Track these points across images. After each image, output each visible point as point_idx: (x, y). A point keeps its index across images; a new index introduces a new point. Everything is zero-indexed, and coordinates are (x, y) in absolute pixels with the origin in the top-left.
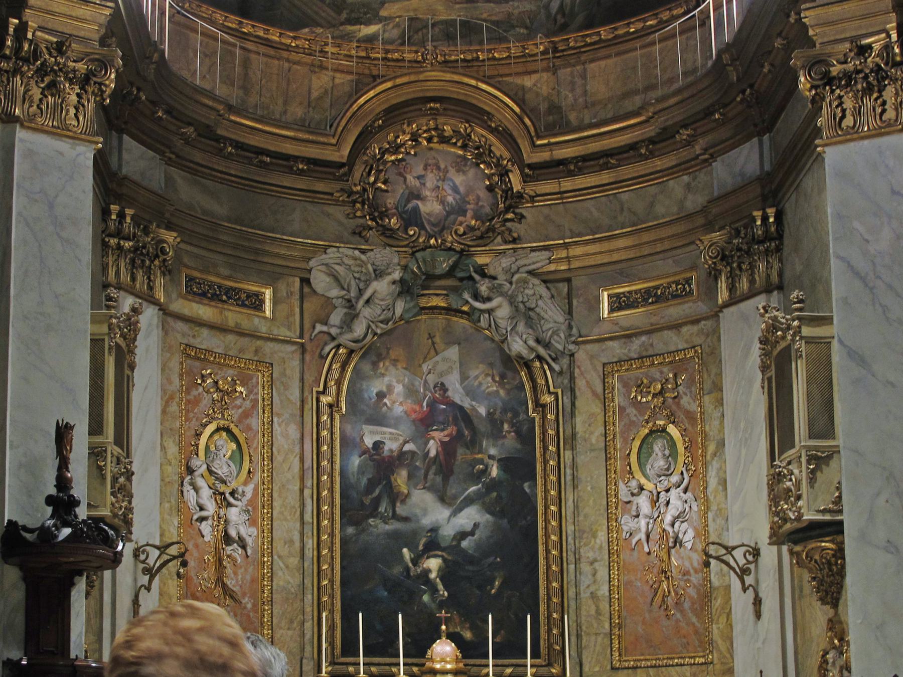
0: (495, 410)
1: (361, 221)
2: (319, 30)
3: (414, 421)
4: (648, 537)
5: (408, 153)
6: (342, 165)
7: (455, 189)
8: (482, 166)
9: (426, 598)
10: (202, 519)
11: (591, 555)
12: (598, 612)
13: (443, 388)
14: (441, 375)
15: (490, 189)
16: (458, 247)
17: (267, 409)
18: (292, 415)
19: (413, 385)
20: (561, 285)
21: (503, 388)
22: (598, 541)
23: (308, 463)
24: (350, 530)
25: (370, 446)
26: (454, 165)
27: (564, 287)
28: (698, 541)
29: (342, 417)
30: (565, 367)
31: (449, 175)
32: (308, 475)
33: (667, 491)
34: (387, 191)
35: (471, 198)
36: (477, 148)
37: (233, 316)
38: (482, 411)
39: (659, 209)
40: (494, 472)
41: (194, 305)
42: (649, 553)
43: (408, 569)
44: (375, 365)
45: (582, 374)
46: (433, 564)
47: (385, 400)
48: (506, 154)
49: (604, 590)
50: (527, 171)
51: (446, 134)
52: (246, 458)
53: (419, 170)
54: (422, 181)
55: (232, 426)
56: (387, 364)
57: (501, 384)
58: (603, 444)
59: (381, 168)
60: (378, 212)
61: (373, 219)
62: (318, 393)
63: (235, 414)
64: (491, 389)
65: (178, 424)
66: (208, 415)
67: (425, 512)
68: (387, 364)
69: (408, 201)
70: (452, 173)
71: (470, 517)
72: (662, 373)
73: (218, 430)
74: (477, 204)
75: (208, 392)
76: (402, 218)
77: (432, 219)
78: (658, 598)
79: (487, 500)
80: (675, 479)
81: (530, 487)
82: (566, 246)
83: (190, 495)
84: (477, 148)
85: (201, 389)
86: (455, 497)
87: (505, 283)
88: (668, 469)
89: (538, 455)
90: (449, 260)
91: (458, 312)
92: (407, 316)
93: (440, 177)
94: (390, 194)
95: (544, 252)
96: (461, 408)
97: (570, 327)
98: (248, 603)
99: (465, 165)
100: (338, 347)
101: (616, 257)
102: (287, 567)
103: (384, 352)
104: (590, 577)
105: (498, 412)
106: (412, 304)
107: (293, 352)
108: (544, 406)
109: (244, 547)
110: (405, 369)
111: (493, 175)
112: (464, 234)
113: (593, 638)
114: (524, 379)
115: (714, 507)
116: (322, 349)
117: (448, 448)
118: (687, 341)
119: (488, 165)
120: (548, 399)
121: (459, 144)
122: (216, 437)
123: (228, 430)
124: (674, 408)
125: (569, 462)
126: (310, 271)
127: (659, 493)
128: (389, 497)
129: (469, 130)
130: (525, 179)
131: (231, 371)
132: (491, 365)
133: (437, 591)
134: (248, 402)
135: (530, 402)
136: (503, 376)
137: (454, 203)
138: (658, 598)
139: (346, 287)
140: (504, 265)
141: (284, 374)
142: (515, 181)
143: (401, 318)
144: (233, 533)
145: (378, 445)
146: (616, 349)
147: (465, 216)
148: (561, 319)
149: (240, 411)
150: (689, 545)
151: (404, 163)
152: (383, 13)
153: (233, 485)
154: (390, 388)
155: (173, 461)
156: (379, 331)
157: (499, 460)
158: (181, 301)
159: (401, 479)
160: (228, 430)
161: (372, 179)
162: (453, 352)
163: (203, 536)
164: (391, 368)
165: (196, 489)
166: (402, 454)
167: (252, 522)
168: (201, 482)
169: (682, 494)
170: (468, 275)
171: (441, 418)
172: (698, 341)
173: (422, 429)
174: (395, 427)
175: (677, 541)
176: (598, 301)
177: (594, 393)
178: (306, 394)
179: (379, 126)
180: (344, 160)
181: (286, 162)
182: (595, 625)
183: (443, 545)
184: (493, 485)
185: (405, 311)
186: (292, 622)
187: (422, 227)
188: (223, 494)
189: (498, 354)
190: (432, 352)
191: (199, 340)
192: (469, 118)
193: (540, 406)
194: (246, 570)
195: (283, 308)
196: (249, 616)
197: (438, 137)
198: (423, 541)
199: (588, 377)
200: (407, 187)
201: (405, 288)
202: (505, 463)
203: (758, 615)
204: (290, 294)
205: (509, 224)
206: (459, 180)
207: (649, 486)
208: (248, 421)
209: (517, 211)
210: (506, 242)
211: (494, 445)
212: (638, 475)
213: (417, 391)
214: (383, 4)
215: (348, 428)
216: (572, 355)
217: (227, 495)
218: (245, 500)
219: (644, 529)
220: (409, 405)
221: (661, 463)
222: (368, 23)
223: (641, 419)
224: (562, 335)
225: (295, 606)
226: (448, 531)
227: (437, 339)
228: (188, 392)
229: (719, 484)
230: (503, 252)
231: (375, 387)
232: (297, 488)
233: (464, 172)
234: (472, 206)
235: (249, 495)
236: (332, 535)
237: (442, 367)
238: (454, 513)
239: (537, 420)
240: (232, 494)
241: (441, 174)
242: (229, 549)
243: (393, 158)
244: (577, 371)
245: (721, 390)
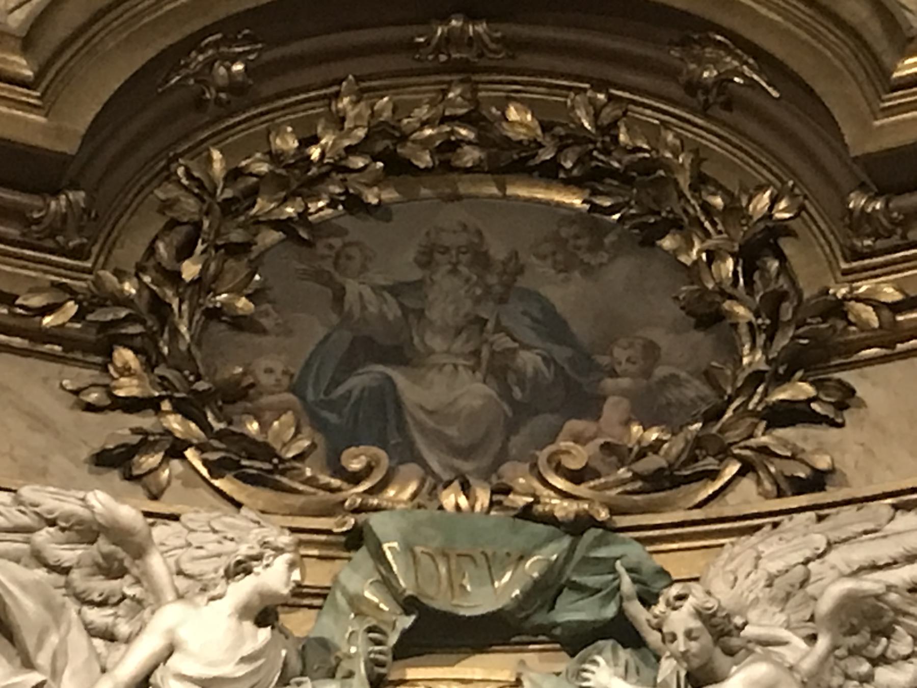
26: (547, 248)
54: (410, 303)
74: (647, 374)
77: (452, 431)
87: (785, 634)
90: (522, 558)
93: (488, 289)
99: (596, 247)
137: (548, 374)
151: (337, 242)
170: (610, 611)
179: (235, 87)
192: (611, 72)
197: (479, 143)
200: (346, 318)
233: (588, 270)
241: (492, 279)
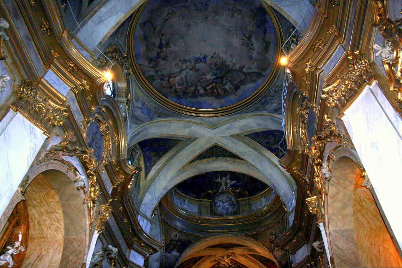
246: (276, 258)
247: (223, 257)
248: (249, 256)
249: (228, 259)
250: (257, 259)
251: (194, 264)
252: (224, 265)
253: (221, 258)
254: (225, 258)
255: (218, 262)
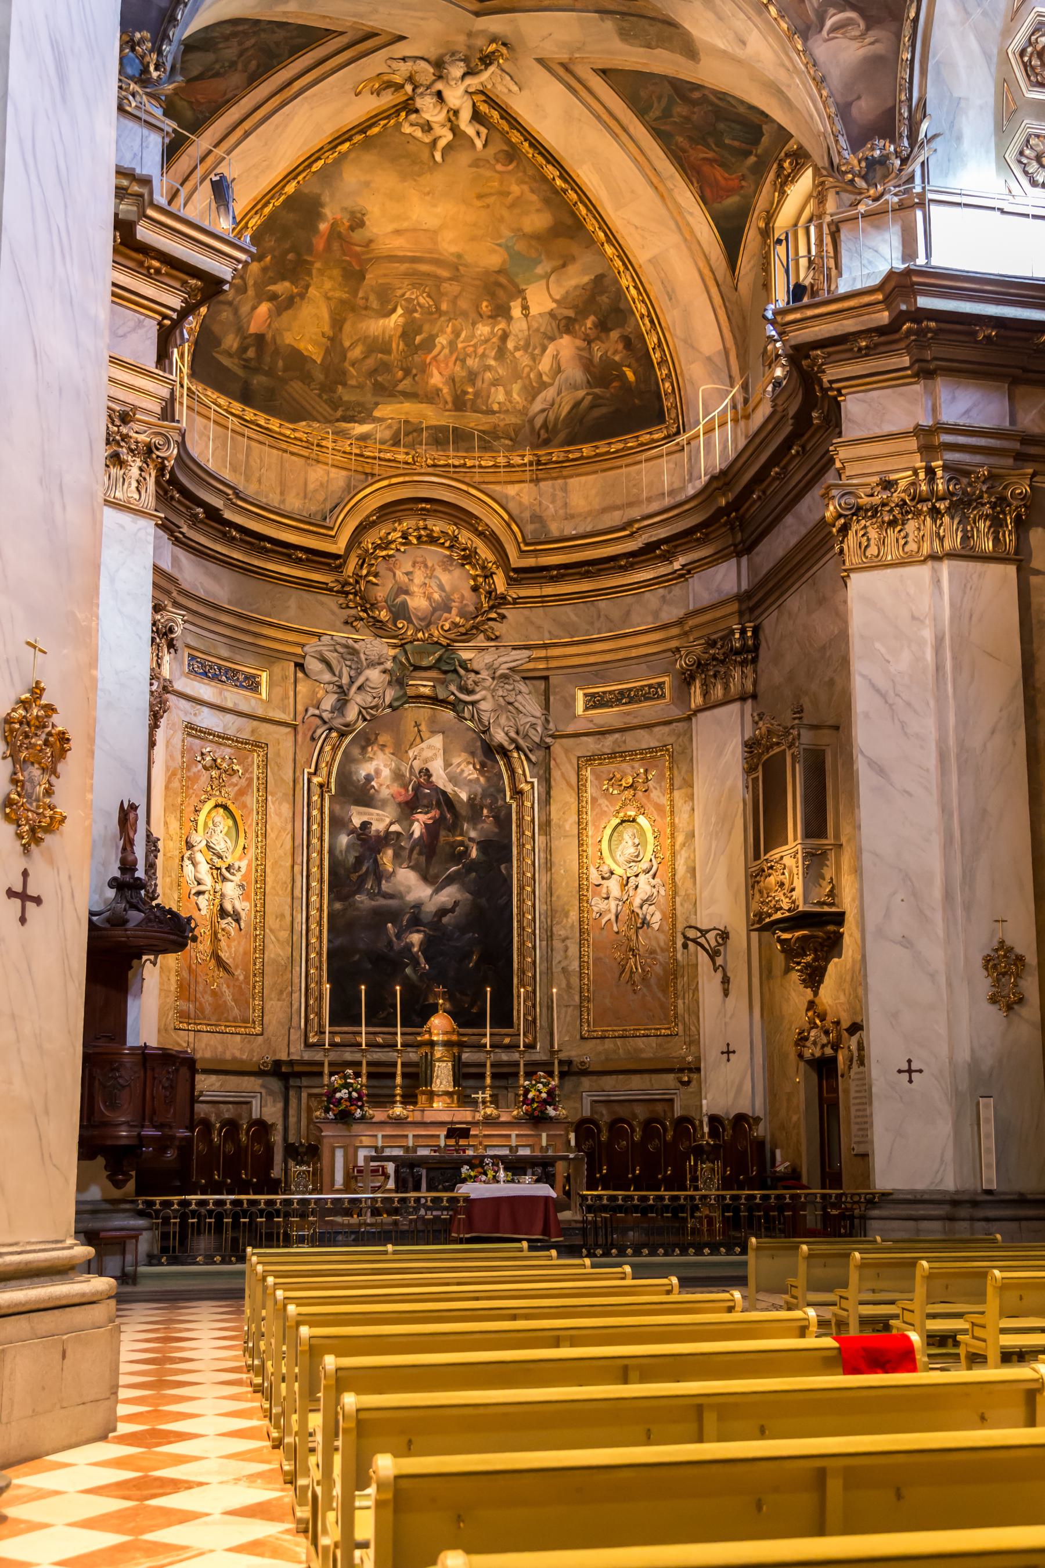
0: (476, 795)
1: (353, 612)
2: (316, 425)
3: (400, 804)
4: (617, 917)
5: (398, 550)
6: (337, 557)
7: (441, 587)
8: (467, 567)
9: (408, 970)
10: (199, 893)
11: (562, 933)
12: (569, 986)
13: (427, 773)
14: (426, 761)
15: (475, 589)
16: (444, 642)
17: (262, 787)
18: (284, 794)
19: (400, 770)
20: (537, 683)
21: (483, 776)
22: (570, 920)
23: (298, 841)
24: (338, 906)
25: (358, 826)
27: (541, 685)
28: (664, 923)
29: (331, 797)
30: (541, 758)
31: (436, 573)
32: (298, 851)
33: (637, 876)
34: (376, 584)
35: (456, 596)
36: (464, 550)
37: (234, 697)
38: (464, 796)
39: (635, 617)
40: (474, 854)
41: (196, 683)
42: (617, 933)
43: (390, 943)
44: (364, 749)
45: (557, 764)
46: (416, 938)
47: (373, 783)
48: (491, 558)
49: (575, 966)
50: (512, 574)
51: (435, 535)
52: (242, 834)
53: (408, 568)
55: (229, 804)
56: (375, 748)
57: (481, 772)
58: (576, 832)
59: (373, 562)
60: (368, 604)
61: (365, 611)
62: (309, 773)
63: (232, 791)
64: (471, 777)
65: (179, 800)
66: (206, 792)
67: (409, 889)
68: (375, 748)
69: (397, 595)
70: (439, 572)
71: (449, 895)
72: (633, 768)
73: (216, 806)
75: (205, 768)
76: (391, 611)
78: (626, 976)
79: (467, 880)
80: (644, 865)
81: (506, 868)
82: (545, 646)
83: (189, 868)
84: (464, 550)
85: (200, 766)
86: (437, 877)
88: (637, 856)
89: (514, 839)
91: (443, 702)
92: (396, 704)
94: (379, 588)
95: (524, 651)
96: (444, 793)
97: (547, 721)
98: (239, 973)
99: (451, 565)
100: (330, 729)
101: (592, 659)
102: (278, 940)
103: (373, 738)
104: (562, 953)
105: (478, 799)
106: (401, 693)
107: (287, 734)
108: (521, 793)
109: (238, 921)
110: (393, 754)
111: (477, 576)
112: (449, 630)
113: (564, 1009)
114: (503, 768)
115: (682, 893)
116: (314, 732)
117: (431, 830)
118: (658, 740)
119: (474, 567)
120: (526, 787)
121: (447, 544)
122: (213, 814)
123: (225, 808)
124: (644, 801)
125: (543, 846)
126: (304, 657)
127: (628, 878)
128: (375, 874)
129: (456, 533)
130: (511, 582)
131: (229, 750)
132: (473, 754)
133: (418, 963)
134: (243, 780)
135: (507, 789)
136: (483, 765)
138: (626, 976)
139: (337, 673)
140: (487, 661)
141: (278, 754)
142: (500, 583)
143: (390, 706)
144: (229, 907)
145: (365, 825)
146: (590, 745)
147: (450, 612)
148: (538, 714)
149: (236, 788)
150: (656, 926)
152: (377, 414)
153: (229, 860)
154: (378, 772)
155: (174, 837)
156: (368, 718)
157: (478, 843)
158: (184, 680)
159: (387, 857)
160: (225, 808)
161: (364, 572)
162: (437, 741)
163: (200, 910)
164: (380, 754)
165: (194, 864)
166: (387, 833)
167: (245, 896)
168: (199, 857)
169: (651, 880)
171: (425, 802)
172: (671, 740)
173: (408, 811)
174: (382, 808)
175: (645, 923)
176: (574, 698)
177: (569, 784)
178: (298, 774)
180: (342, 552)
181: (285, 551)
182: (566, 997)
183: (425, 921)
184: (472, 866)
185: (396, 699)
186: (281, 992)
187: (410, 621)
188: (218, 869)
189: (479, 744)
190: (418, 739)
191: (200, 718)
193: (518, 793)
194: (239, 943)
195: (278, 691)
196: (241, 987)
198: (407, 916)
199: (563, 770)
200: (396, 582)
201: (398, 681)
202: (484, 846)
203: (726, 993)
204: (285, 678)
205: (491, 623)
206: (445, 578)
207: (619, 871)
208: (244, 798)
209: (499, 611)
210: (489, 639)
211: (474, 829)
212: (609, 861)
213: (403, 776)
214: (377, 404)
215: (337, 808)
216: (548, 748)
217: (224, 871)
218: (239, 875)
219: (613, 911)
220: (395, 788)
221: (632, 850)
222: (361, 422)
223: (612, 809)
224: (539, 729)
225: (285, 977)
226: (430, 908)
227: (423, 728)
228: (188, 769)
229: (687, 871)
230: (486, 648)
231: (364, 770)
232: (289, 863)
233: (450, 571)
234: (456, 604)
235: (243, 870)
236: (320, 910)
237: (427, 754)
238: (437, 891)
239: (514, 806)
240: (228, 869)
242: (223, 923)
243: (384, 553)
244: (552, 763)
245: (691, 786)
246: (821, 82)
247: (439, 65)
248: (598, 84)
249: (469, 81)
250: (641, 110)
251: (254, 79)
252: (427, 127)
253: (423, 64)
254: (457, 70)
255: (400, 97)
